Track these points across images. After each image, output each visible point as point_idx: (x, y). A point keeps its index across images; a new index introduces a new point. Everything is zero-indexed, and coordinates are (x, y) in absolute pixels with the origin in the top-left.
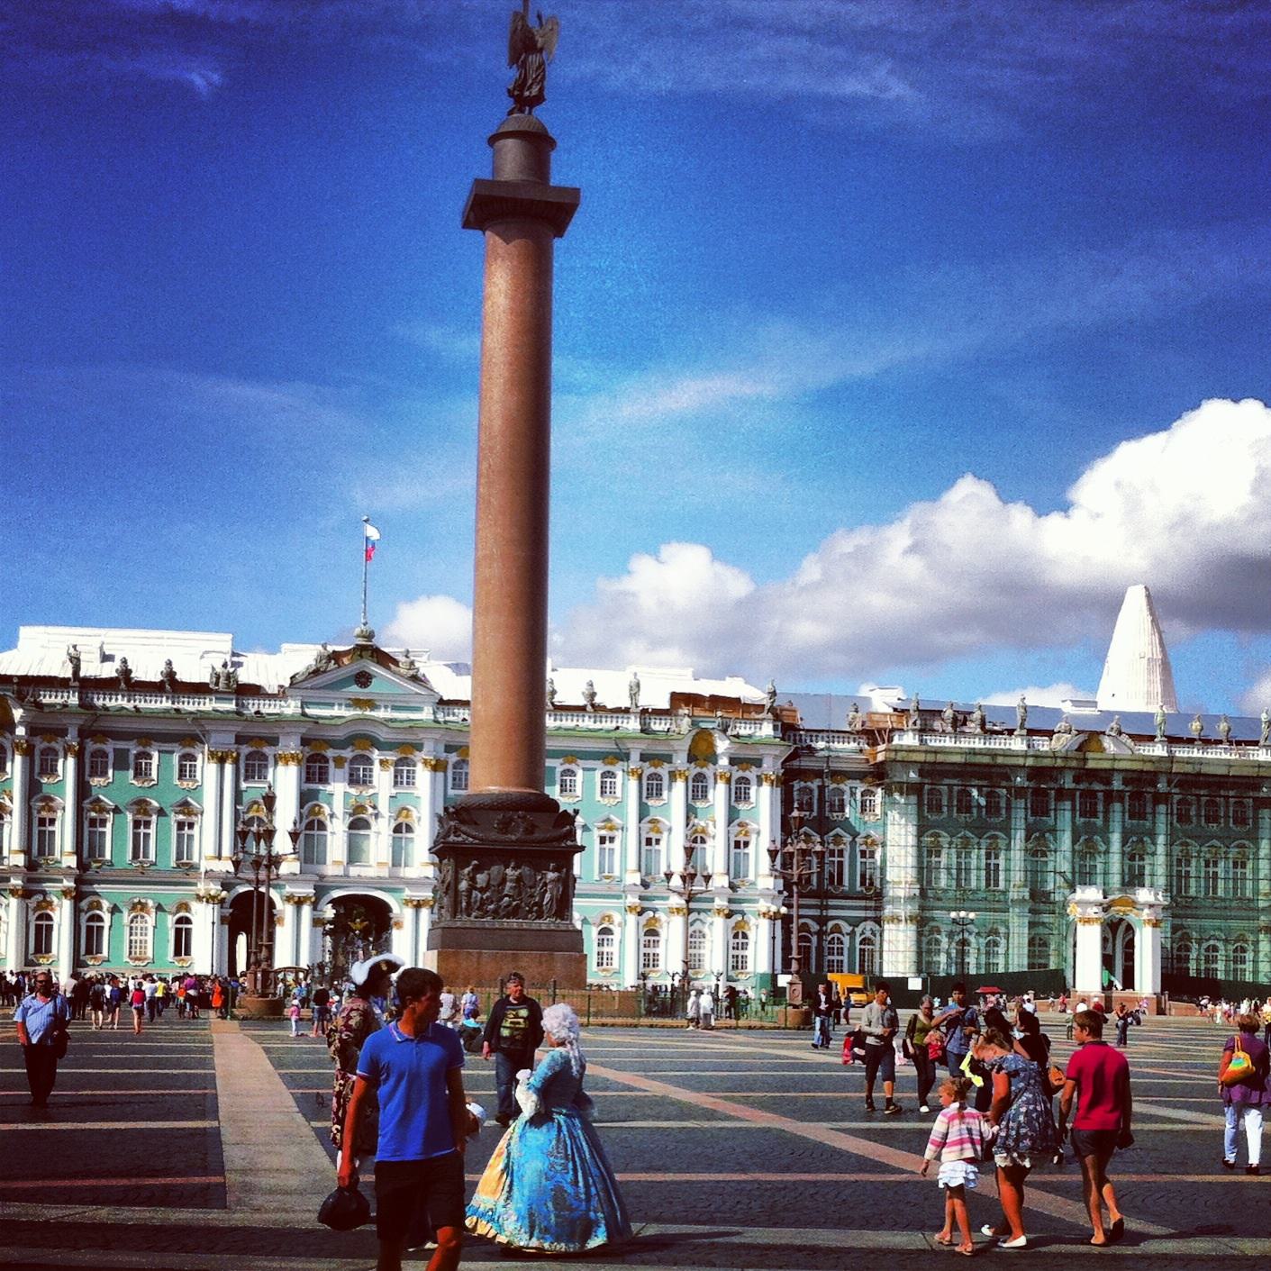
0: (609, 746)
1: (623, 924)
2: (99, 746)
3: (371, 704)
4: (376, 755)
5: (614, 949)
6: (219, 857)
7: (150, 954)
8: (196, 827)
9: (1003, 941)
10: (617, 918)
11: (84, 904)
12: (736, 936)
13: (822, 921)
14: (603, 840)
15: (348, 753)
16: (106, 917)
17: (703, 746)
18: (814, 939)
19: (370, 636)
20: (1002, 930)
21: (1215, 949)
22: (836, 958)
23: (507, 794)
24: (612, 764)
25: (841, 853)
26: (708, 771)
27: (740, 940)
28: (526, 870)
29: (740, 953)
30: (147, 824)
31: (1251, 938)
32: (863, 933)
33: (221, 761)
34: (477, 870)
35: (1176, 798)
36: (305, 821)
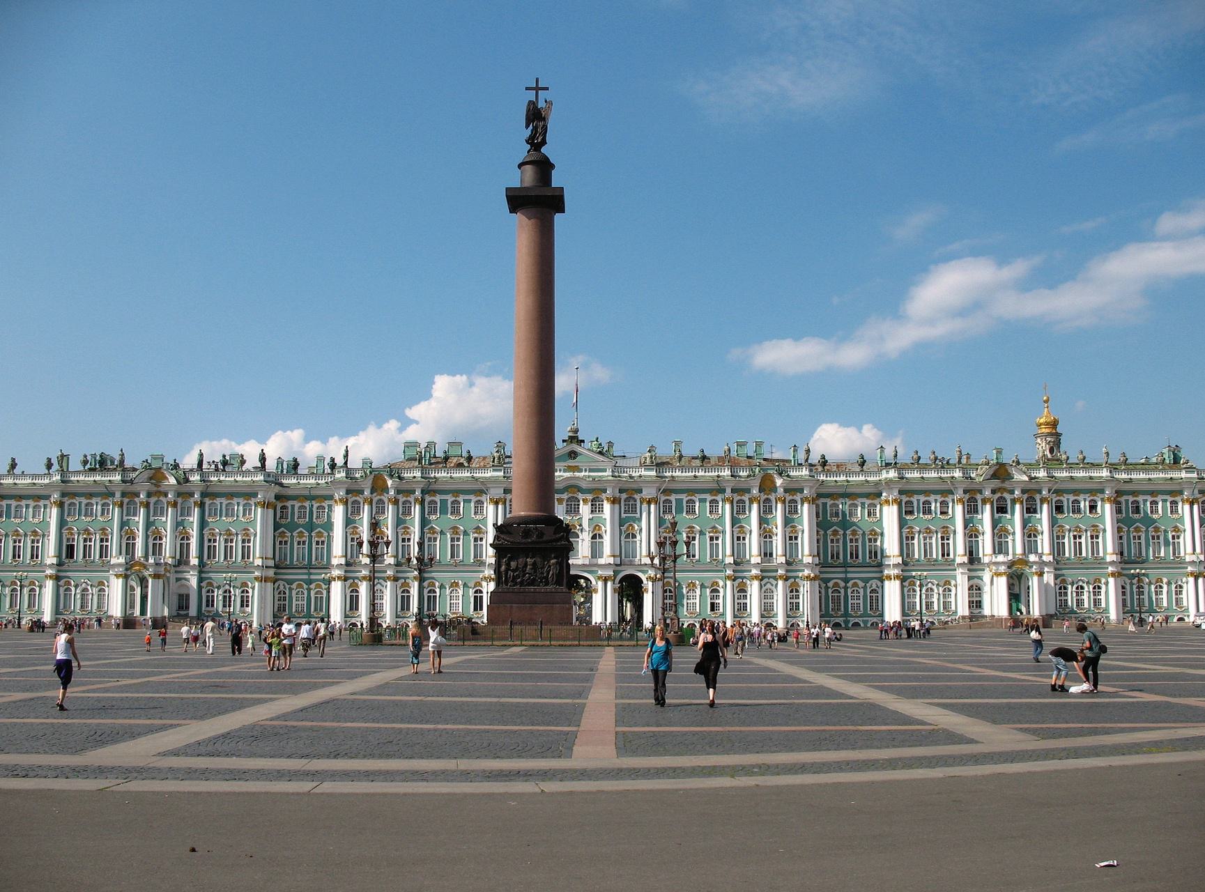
3: (578, 469)
5: (720, 601)
10: (721, 583)
11: (425, 584)
13: (846, 580)
15: (565, 496)
16: (438, 590)
17: (768, 483)
18: (842, 591)
19: (576, 431)
20: (953, 582)
21: (1082, 588)
25: (857, 540)
26: (772, 497)
29: (742, 601)
30: (458, 539)
33: (496, 503)
34: (511, 559)
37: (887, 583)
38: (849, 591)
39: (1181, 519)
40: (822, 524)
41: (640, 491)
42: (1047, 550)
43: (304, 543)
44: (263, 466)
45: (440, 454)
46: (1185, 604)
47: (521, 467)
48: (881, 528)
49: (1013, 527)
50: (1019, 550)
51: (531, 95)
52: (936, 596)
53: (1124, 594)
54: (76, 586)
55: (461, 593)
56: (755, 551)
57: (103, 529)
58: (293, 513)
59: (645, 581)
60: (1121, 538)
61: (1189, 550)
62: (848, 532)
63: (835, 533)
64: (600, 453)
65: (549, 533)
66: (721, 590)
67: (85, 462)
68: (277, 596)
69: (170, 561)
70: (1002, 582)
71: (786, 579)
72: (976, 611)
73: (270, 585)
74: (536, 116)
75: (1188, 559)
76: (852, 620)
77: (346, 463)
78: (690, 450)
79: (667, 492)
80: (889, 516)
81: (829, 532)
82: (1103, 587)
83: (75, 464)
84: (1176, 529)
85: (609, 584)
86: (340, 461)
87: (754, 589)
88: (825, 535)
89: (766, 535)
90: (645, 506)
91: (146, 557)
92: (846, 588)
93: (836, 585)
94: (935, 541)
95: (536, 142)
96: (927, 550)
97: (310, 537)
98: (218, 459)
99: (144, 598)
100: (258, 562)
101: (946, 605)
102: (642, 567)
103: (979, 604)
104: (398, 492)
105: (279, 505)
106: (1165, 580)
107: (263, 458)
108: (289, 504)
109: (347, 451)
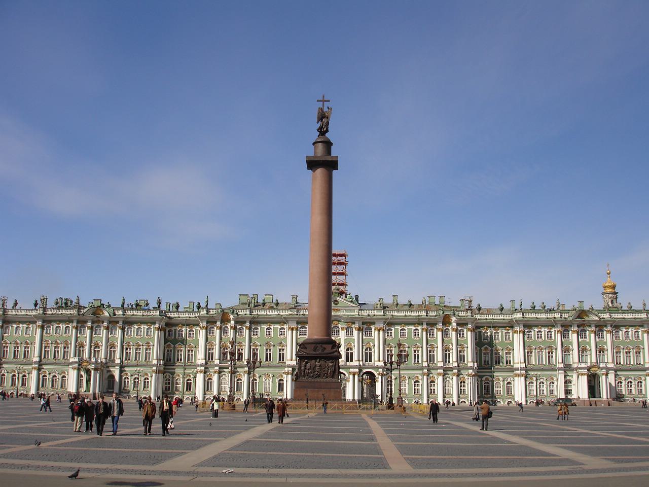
0: (417, 321)
1: (422, 380)
2: (256, 326)
4: (340, 326)
6: (292, 360)
7: (271, 391)
8: (285, 351)
10: (420, 377)
16: (258, 379)
17: (447, 320)
18: (490, 383)
22: (498, 389)
23: (320, 339)
24: (417, 326)
27: (463, 384)
28: (322, 362)
33: (292, 329)
37: (516, 378)
44: (159, 306)
45: (260, 301)
47: (312, 311)
48: (513, 346)
49: (590, 347)
50: (594, 360)
51: (320, 105)
52: (545, 386)
54: (50, 374)
55: (271, 380)
56: (440, 358)
57: (66, 341)
58: (175, 334)
59: (376, 375)
63: (486, 348)
64: (351, 301)
65: (328, 348)
66: (420, 381)
67: (57, 303)
68: (165, 380)
69: (104, 361)
70: (584, 380)
73: (161, 375)
74: (323, 117)
77: (207, 306)
78: (402, 300)
80: (518, 340)
81: (483, 348)
82: (643, 382)
83: (51, 304)
85: (356, 377)
86: (203, 305)
87: (439, 381)
88: (480, 350)
89: (446, 350)
90: (376, 332)
91: (90, 358)
92: (492, 381)
93: (487, 379)
94: (544, 354)
95: (323, 131)
96: (540, 359)
98: (134, 302)
100: (155, 362)
101: (551, 392)
102: (377, 368)
104: (237, 322)
105: (168, 329)
107: (159, 303)
108: (173, 328)
109: (208, 299)
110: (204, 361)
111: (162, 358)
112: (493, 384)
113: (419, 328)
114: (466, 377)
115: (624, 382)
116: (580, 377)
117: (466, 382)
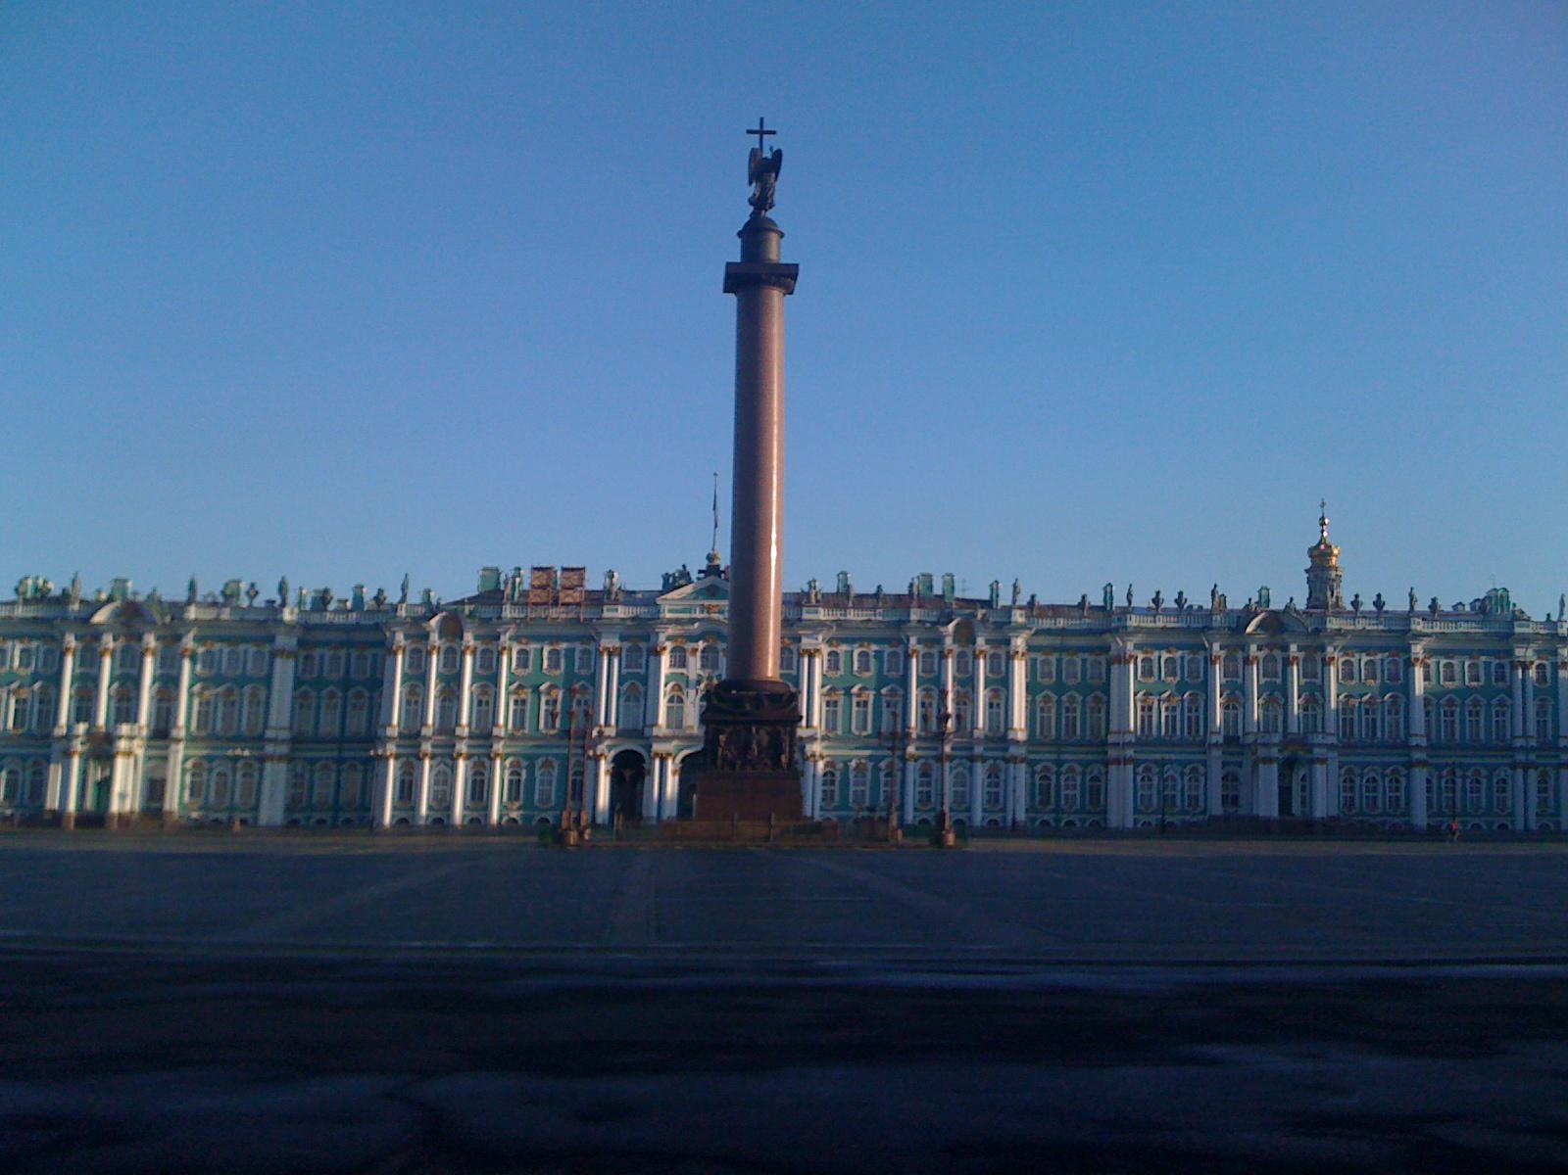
1: (903, 770)
9: (1203, 779)
12: (989, 777)
13: (1059, 763)
14: (888, 705)
15: (701, 645)
18: (1053, 777)
20: (1202, 769)
21: (1374, 780)
25: (1075, 710)
26: (969, 650)
31: (1403, 771)
32: (1091, 773)
35: (1341, 660)
36: (668, 697)
37: (1113, 768)
38: (1063, 778)
39: (1511, 696)
40: (1031, 688)
41: (798, 640)
42: (1331, 727)
43: (336, 706)
46: (1509, 803)
52: (1179, 787)
53: (1429, 790)
60: (1427, 714)
61: (1519, 733)
62: (1064, 698)
71: (984, 762)
72: (1231, 810)
75: (1519, 742)
76: (1066, 818)
79: (829, 642)
82: (1403, 780)
84: (1501, 703)
86: (393, 596)
92: (1058, 774)
93: (1045, 768)
95: (762, 202)
97: (345, 698)
99: (105, 786)
103: (1235, 800)
105: (302, 654)
106: (1484, 772)
107: (282, 588)
108: (317, 652)
110: (1425, 739)
111: (286, 723)
112: (1058, 779)
113: (900, 650)
114: (1001, 764)
115: (1358, 782)
116: (1261, 766)
117: (1002, 778)
